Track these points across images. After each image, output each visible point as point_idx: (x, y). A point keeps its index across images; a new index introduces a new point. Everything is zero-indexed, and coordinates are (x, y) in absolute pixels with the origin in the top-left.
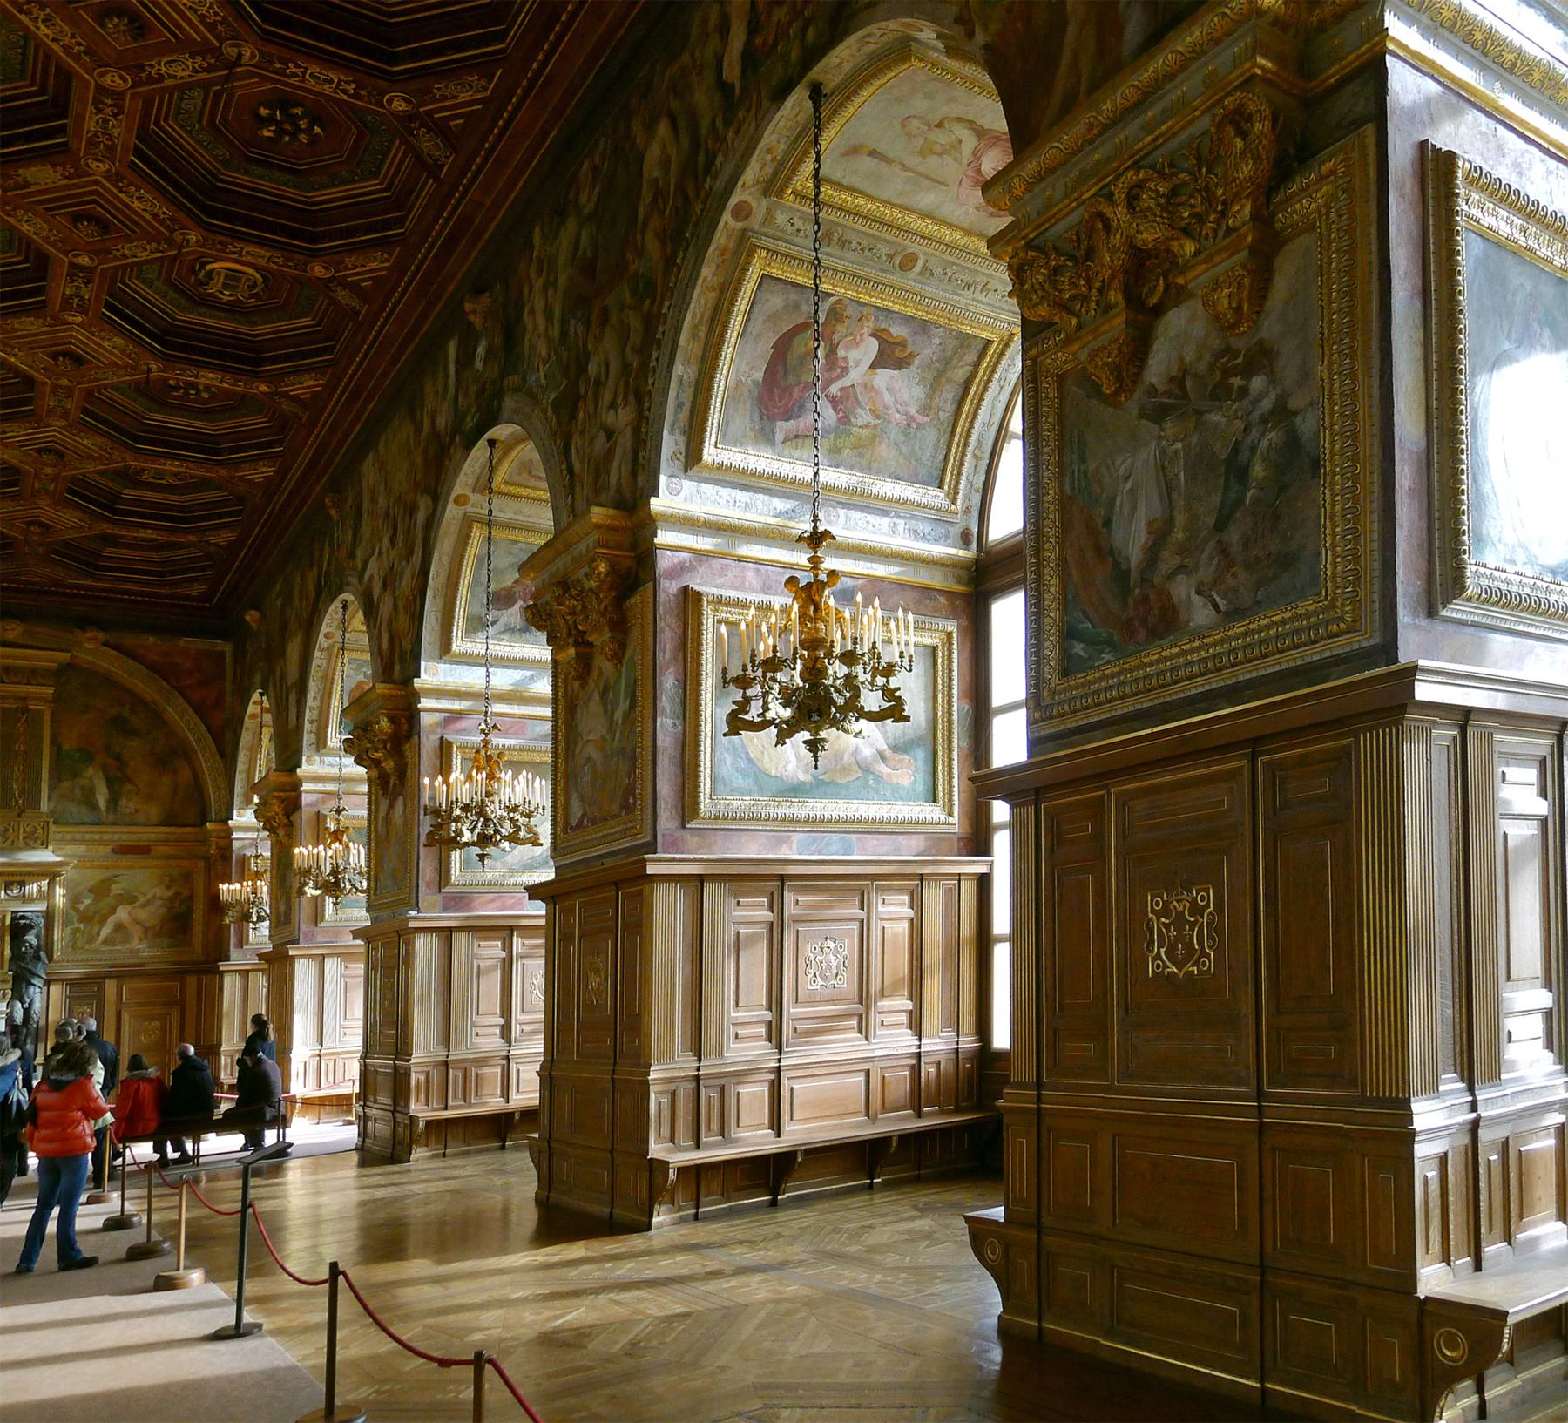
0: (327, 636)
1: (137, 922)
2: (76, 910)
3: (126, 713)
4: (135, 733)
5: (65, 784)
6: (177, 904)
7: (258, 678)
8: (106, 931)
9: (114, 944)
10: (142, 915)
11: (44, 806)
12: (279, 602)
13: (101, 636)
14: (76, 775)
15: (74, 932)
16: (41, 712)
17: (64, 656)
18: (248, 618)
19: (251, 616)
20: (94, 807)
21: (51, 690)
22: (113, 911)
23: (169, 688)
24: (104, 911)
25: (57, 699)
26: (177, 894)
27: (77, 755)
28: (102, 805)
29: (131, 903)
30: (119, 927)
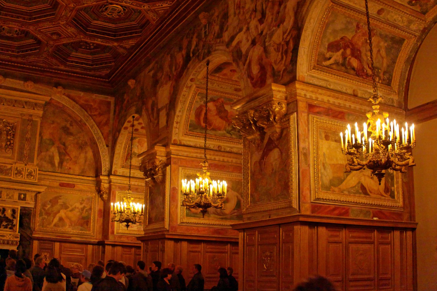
0: (192, 80)
1: (68, 217)
2: (44, 209)
3: (68, 125)
4: (71, 134)
5: (43, 154)
6: (85, 211)
7: (134, 109)
8: (56, 220)
9: (59, 227)
10: (70, 214)
11: (36, 162)
12: (152, 72)
13: (63, 91)
14: (47, 150)
15: (43, 219)
16: (36, 121)
17: (48, 99)
18: (129, 83)
19: (131, 83)
20: (53, 164)
21: (41, 113)
22: (59, 212)
23: (88, 115)
24: (55, 212)
25: (44, 117)
26: (84, 207)
27: (48, 142)
28: (57, 164)
29: (66, 209)
30: (61, 219)
